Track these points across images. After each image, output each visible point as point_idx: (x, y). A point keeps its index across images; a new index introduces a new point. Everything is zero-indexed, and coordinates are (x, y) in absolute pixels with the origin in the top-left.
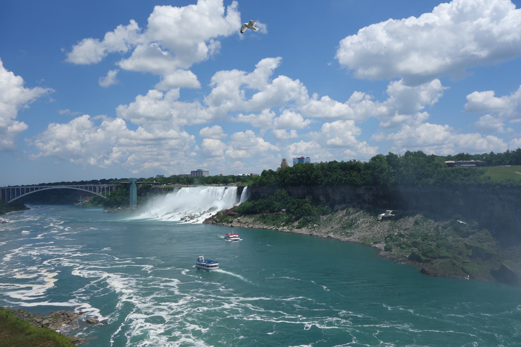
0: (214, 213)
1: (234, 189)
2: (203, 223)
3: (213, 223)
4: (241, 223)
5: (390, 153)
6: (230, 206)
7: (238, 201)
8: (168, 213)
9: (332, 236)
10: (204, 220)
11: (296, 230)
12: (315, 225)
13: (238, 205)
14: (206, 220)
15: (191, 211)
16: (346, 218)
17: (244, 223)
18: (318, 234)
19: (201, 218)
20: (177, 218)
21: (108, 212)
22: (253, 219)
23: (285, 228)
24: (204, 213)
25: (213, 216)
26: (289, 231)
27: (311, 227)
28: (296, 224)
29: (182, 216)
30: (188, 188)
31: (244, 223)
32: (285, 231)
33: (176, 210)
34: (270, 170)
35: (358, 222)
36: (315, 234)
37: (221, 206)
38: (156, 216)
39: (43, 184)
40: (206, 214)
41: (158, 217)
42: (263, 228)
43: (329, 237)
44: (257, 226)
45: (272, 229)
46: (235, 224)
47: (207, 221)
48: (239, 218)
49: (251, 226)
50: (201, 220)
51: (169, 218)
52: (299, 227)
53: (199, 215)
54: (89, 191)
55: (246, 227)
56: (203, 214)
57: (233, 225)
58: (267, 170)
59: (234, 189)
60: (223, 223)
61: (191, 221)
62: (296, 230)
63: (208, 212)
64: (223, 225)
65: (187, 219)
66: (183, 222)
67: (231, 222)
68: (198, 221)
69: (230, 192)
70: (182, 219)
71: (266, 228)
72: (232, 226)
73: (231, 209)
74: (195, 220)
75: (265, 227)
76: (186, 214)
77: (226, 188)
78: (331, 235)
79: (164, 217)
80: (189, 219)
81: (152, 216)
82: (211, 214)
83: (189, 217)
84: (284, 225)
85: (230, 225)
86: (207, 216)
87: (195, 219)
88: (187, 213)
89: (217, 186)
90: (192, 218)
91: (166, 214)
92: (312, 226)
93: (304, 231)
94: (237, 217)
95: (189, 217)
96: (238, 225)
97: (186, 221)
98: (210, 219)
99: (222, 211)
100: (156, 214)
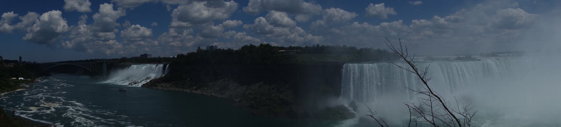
0: (148, 81)
1: (161, 66)
2: (141, 86)
3: (147, 87)
4: (163, 87)
5: (251, 44)
6: (159, 76)
7: (164, 74)
8: (123, 80)
9: (214, 95)
10: (142, 85)
11: (194, 91)
12: (205, 88)
13: (163, 76)
14: (143, 85)
15: (136, 79)
16: (223, 84)
17: (165, 87)
18: (206, 94)
19: (141, 83)
20: (127, 84)
21: (91, 78)
22: (170, 84)
23: (188, 90)
24: (143, 80)
25: (148, 82)
26: (190, 92)
27: (202, 89)
28: (195, 87)
29: (130, 82)
30: (136, 65)
31: (165, 87)
32: (187, 92)
33: (128, 79)
34: (182, 54)
35: (230, 86)
36: (204, 93)
37: (153, 76)
38: (115, 82)
39: (61, 62)
40: (144, 81)
41: (116, 82)
42: (176, 90)
43: (212, 95)
44: (172, 89)
45: (180, 91)
46: (159, 87)
47: (143, 86)
48: (162, 84)
49: (168, 89)
50: (140, 85)
51: (123, 83)
52: (196, 90)
53: (140, 82)
54: (84, 67)
55: (166, 89)
56: (143, 81)
57: (158, 88)
58: (180, 54)
59: (161, 66)
60: (153, 87)
61: (135, 85)
62: (194, 91)
63: (145, 80)
64: (152, 88)
65: (133, 84)
66: (130, 86)
67: (157, 86)
68: (138, 85)
69: (159, 68)
70: (129, 84)
71: (177, 90)
72: (157, 89)
73: (159, 79)
74: (136, 85)
75: (177, 89)
76: (132, 81)
77: (157, 66)
78: (213, 94)
79: (120, 82)
80: (134, 84)
81: (114, 81)
82: (146, 81)
83: (134, 83)
84: (188, 88)
85: (156, 88)
86: (144, 82)
87: (137, 84)
88: (134, 80)
89: (153, 64)
90: (135, 83)
91: (121, 81)
92: (203, 88)
93: (199, 92)
94: (161, 83)
95: (134, 83)
96: (161, 88)
97: (132, 85)
98: (146, 84)
99: (153, 80)
100: (116, 81)
